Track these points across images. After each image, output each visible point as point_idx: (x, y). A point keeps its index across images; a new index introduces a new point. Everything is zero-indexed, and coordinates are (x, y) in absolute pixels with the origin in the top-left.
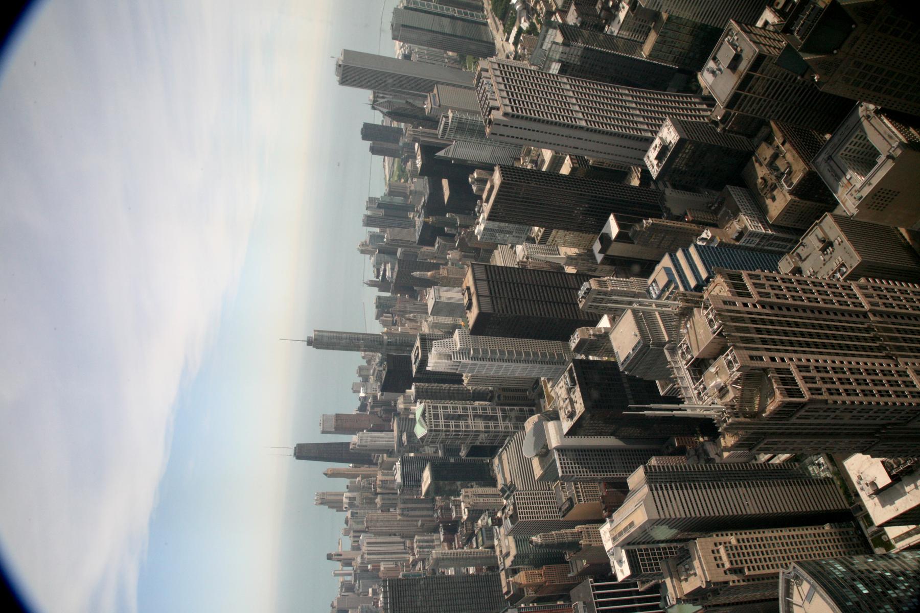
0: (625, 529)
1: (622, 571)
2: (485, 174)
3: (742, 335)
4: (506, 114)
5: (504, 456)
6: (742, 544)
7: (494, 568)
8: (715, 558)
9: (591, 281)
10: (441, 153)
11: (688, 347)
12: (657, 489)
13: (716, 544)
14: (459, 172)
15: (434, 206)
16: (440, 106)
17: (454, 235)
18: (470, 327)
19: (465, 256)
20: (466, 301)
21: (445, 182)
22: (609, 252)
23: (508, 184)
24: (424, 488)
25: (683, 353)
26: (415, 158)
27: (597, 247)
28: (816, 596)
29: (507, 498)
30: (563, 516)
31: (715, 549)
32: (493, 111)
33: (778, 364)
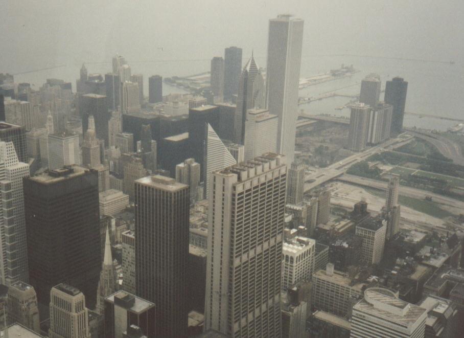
2: (196, 174)
4: (234, 188)
9: (81, 294)
10: (210, 129)
14: (196, 148)
15: (161, 127)
16: (257, 122)
17: (135, 150)
18: (31, 178)
19: (115, 165)
20: (58, 170)
21: (185, 136)
22: (116, 307)
23: (171, 198)
26: (210, 102)
27: (121, 294)
32: (236, 176)
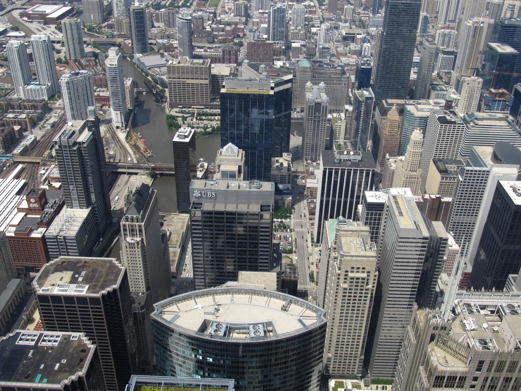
0: (399, 208)
1: (372, 196)
3: (507, 364)
5: (503, 123)
6: (364, 291)
7: (412, 95)
8: (358, 268)
11: (518, 313)
12: (423, 243)
13: (368, 272)
24: (493, 45)
25: (513, 307)
28: (299, 326)
29: (464, 120)
30: (434, 162)
31: (366, 271)
33: (469, 382)
